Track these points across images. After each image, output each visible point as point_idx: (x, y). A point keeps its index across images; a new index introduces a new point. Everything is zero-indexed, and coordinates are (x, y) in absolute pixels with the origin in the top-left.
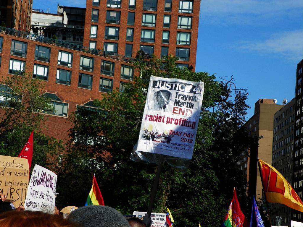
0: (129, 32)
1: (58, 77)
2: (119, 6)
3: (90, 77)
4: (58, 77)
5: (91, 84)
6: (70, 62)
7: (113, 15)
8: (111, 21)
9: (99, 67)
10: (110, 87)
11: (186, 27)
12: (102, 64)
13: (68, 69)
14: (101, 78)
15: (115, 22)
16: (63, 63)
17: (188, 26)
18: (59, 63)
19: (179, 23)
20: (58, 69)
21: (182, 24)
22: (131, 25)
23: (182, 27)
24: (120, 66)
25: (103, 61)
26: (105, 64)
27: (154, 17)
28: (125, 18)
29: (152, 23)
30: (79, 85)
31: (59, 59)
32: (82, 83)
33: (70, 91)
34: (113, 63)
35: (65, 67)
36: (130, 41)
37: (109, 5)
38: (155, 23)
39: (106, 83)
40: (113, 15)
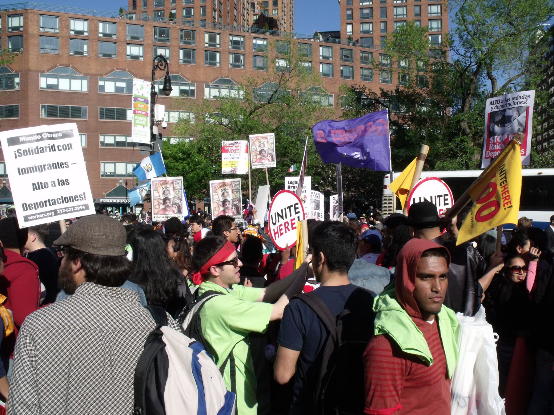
0: (382, 25)
1: (321, 71)
2: (371, 3)
3: (351, 68)
4: (321, 71)
5: (353, 74)
6: (331, 55)
7: (366, 11)
8: (365, 18)
9: (359, 57)
10: (371, 76)
11: (437, 15)
12: (361, 55)
13: (330, 62)
14: (361, 68)
15: (368, 18)
16: (324, 57)
17: (438, 13)
18: (321, 58)
19: (429, 12)
20: (321, 63)
21: (432, 12)
22: (384, 19)
23: (432, 15)
24: (378, 55)
25: (361, 52)
26: (364, 55)
27: (405, 8)
28: (377, 13)
29: (403, 15)
30: (341, 77)
31: (321, 54)
32: (344, 74)
33: (334, 83)
34: (371, 53)
35: (327, 61)
36: (384, 34)
37: (361, 4)
38: (407, 15)
39: (366, 72)
40: (366, 11)
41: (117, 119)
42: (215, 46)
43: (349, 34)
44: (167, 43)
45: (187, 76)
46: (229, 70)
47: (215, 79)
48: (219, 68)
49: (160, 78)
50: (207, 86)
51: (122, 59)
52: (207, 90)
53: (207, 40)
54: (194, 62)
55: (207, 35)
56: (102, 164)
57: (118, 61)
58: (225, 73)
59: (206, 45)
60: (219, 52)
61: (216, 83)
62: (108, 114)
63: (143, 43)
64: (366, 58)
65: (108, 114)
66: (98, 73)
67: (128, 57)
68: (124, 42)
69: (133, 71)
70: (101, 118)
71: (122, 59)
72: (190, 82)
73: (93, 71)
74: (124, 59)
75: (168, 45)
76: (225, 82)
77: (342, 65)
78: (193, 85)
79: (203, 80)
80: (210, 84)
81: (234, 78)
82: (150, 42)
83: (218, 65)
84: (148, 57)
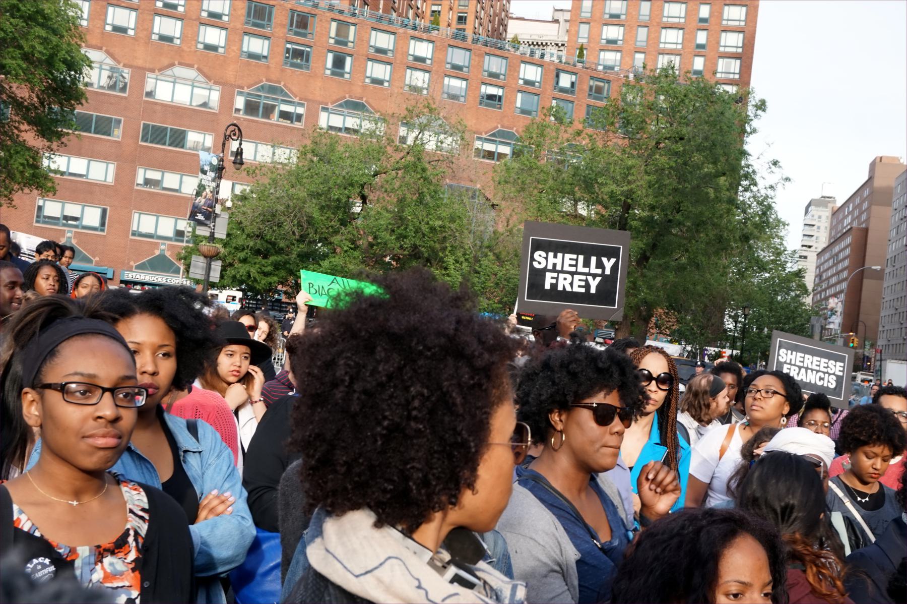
1: (518, 105)
4: (518, 105)
16: (527, 82)
18: (521, 82)
20: (520, 91)
34: (608, 82)
35: (530, 88)
41: (170, 145)
42: (345, 44)
43: (580, 41)
44: (267, 31)
45: (294, 89)
46: (364, 87)
47: (338, 100)
48: (350, 83)
49: (248, 88)
50: (325, 109)
51: (190, 47)
52: (323, 116)
53: (333, 33)
54: (308, 68)
55: (334, 25)
56: (136, 216)
57: (183, 51)
58: (357, 91)
59: (332, 41)
60: (351, 55)
61: (341, 106)
62: (156, 134)
63: (227, 26)
64: (599, 90)
65: (156, 134)
66: (148, 66)
67: (201, 46)
68: (195, 20)
69: (206, 70)
70: (142, 140)
71: (190, 47)
72: (296, 100)
73: (140, 62)
74: (193, 48)
75: (268, 35)
76: (355, 106)
77: (554, 98)
78: (302, 105)
79: (319, 98)
80: (330, 106)
81: (371, 101)
82: (239, 26)
83: (347, 76)
84: (233, 51)
